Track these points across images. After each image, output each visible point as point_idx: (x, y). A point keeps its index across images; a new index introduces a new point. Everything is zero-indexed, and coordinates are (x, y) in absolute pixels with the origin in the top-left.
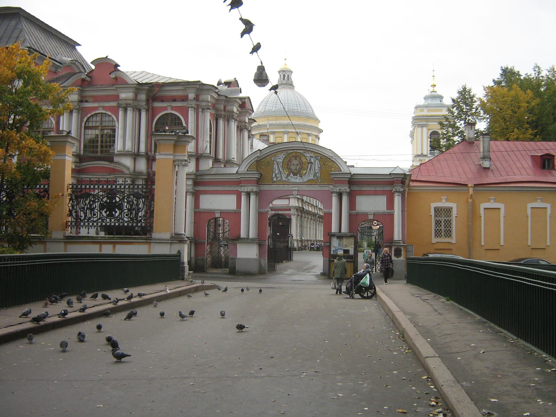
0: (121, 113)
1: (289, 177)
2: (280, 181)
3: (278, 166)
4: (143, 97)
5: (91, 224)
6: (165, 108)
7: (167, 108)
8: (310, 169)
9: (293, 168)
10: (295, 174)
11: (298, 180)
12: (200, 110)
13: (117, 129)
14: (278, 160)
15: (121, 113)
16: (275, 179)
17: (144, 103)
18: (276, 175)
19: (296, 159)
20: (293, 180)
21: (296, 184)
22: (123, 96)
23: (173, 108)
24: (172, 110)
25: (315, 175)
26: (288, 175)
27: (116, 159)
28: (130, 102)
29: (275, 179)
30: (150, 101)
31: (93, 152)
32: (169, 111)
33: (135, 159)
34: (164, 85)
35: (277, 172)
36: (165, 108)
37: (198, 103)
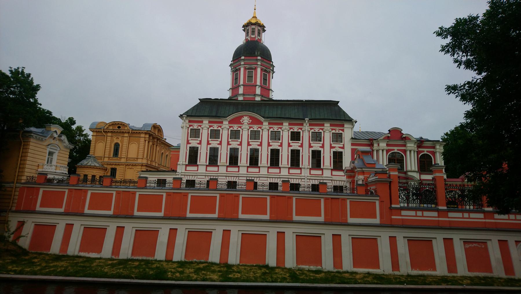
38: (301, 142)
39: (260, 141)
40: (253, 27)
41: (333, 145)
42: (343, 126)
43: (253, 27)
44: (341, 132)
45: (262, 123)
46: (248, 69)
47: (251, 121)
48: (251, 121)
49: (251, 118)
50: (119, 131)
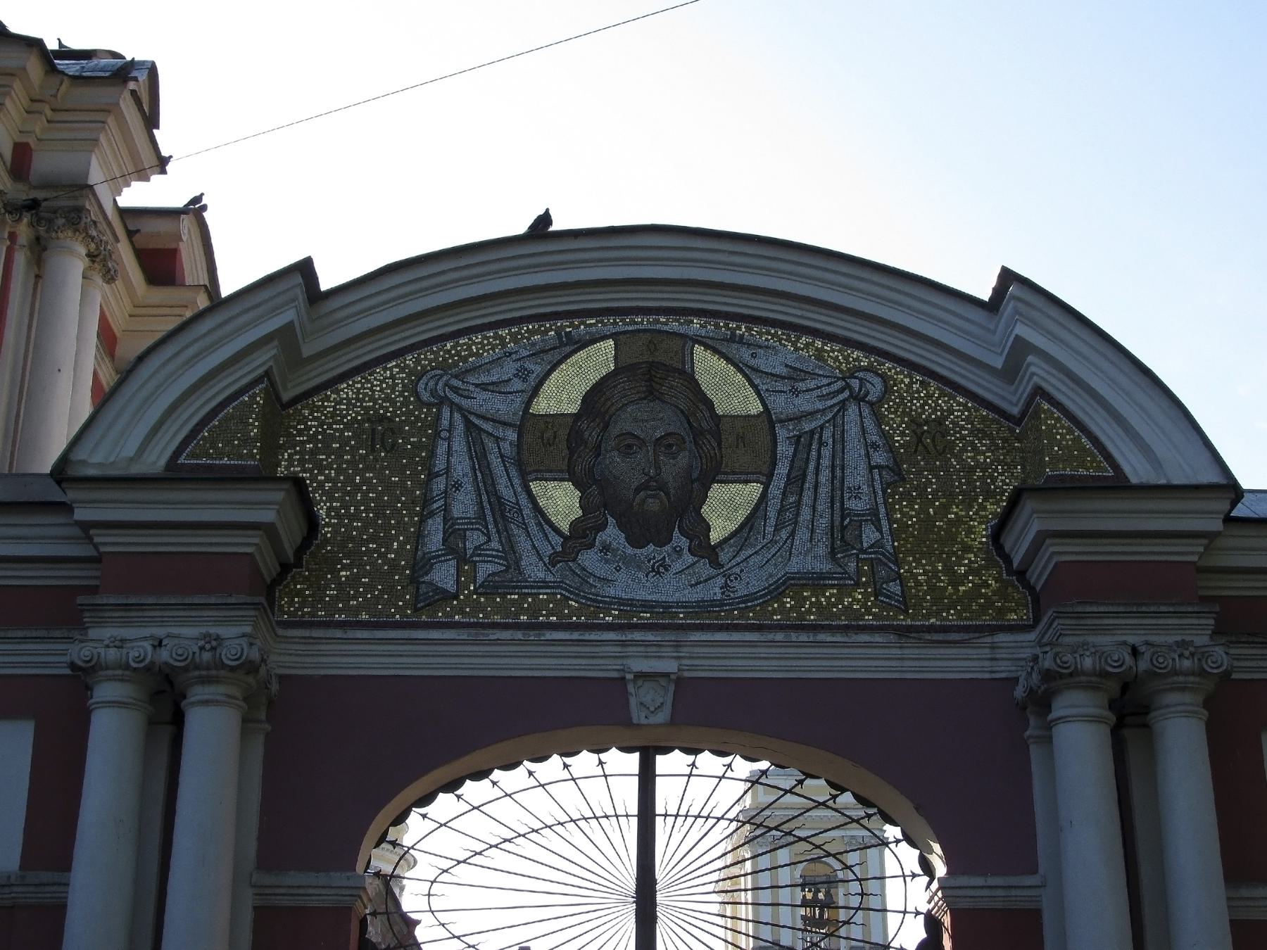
1: (589, 559)
2: (491, 588)
3: (479, 458)
8: (796, 480)
9: (625, 470)
10: (644, 531)
11: (680, 582)
14: (483, 402)
16: (444, 575)
18: (453, 533)
19: (652, 394)
20: (629, 585)
21: (665, 620)
25: (842, 535)
26: (582, 534)
29: (444, 575)
35: (464, 505)
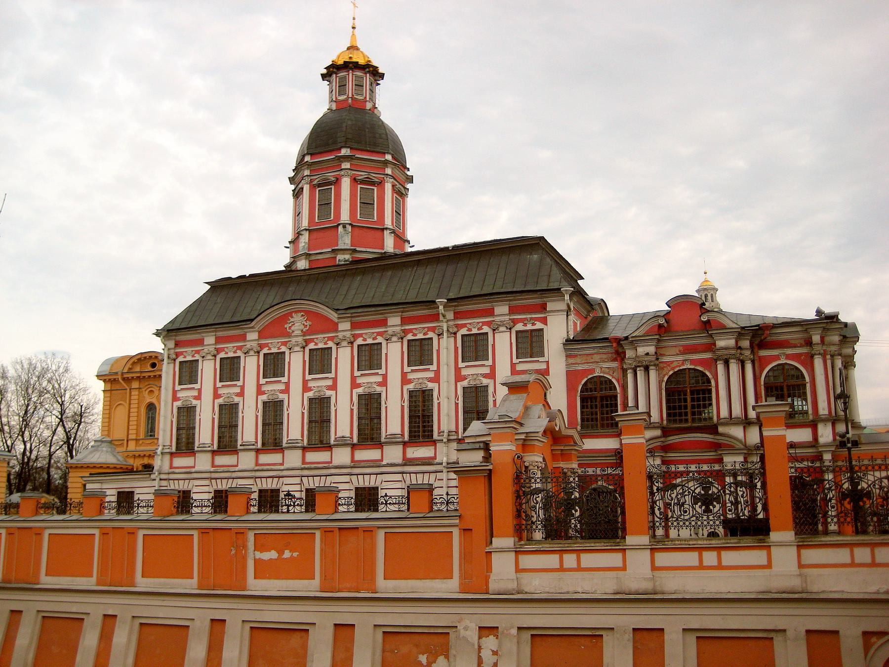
0: (720, 368)
4: (746, 343)
5: (681, 523)
6: (777, 357)
7: (780, 357)
12: (828, 357)
13: (714, 390)
15: (720, 368)
17: (748, 353)
22: (721, 343)
23: (788, 357)
24: (786, 358)
27: (721, 429)
28: (733, 352)
30: (756, 350)
31: (681, 421)
32: (783, 361)
33: (744, 428)
34: (774, 326)
36: (777, 357)
37: (825, 347)
38: (434, 367)
39: (490, 362)
40: (352, 73)
41: (519, 368)
42: (543, 308)
43: (352, 73)
44: (539, 325)
45: (334, 327)
46: (319, 185)
47: (308, 323)
48: (308, 323)
49: (309, 314)
50: (152, 374)
